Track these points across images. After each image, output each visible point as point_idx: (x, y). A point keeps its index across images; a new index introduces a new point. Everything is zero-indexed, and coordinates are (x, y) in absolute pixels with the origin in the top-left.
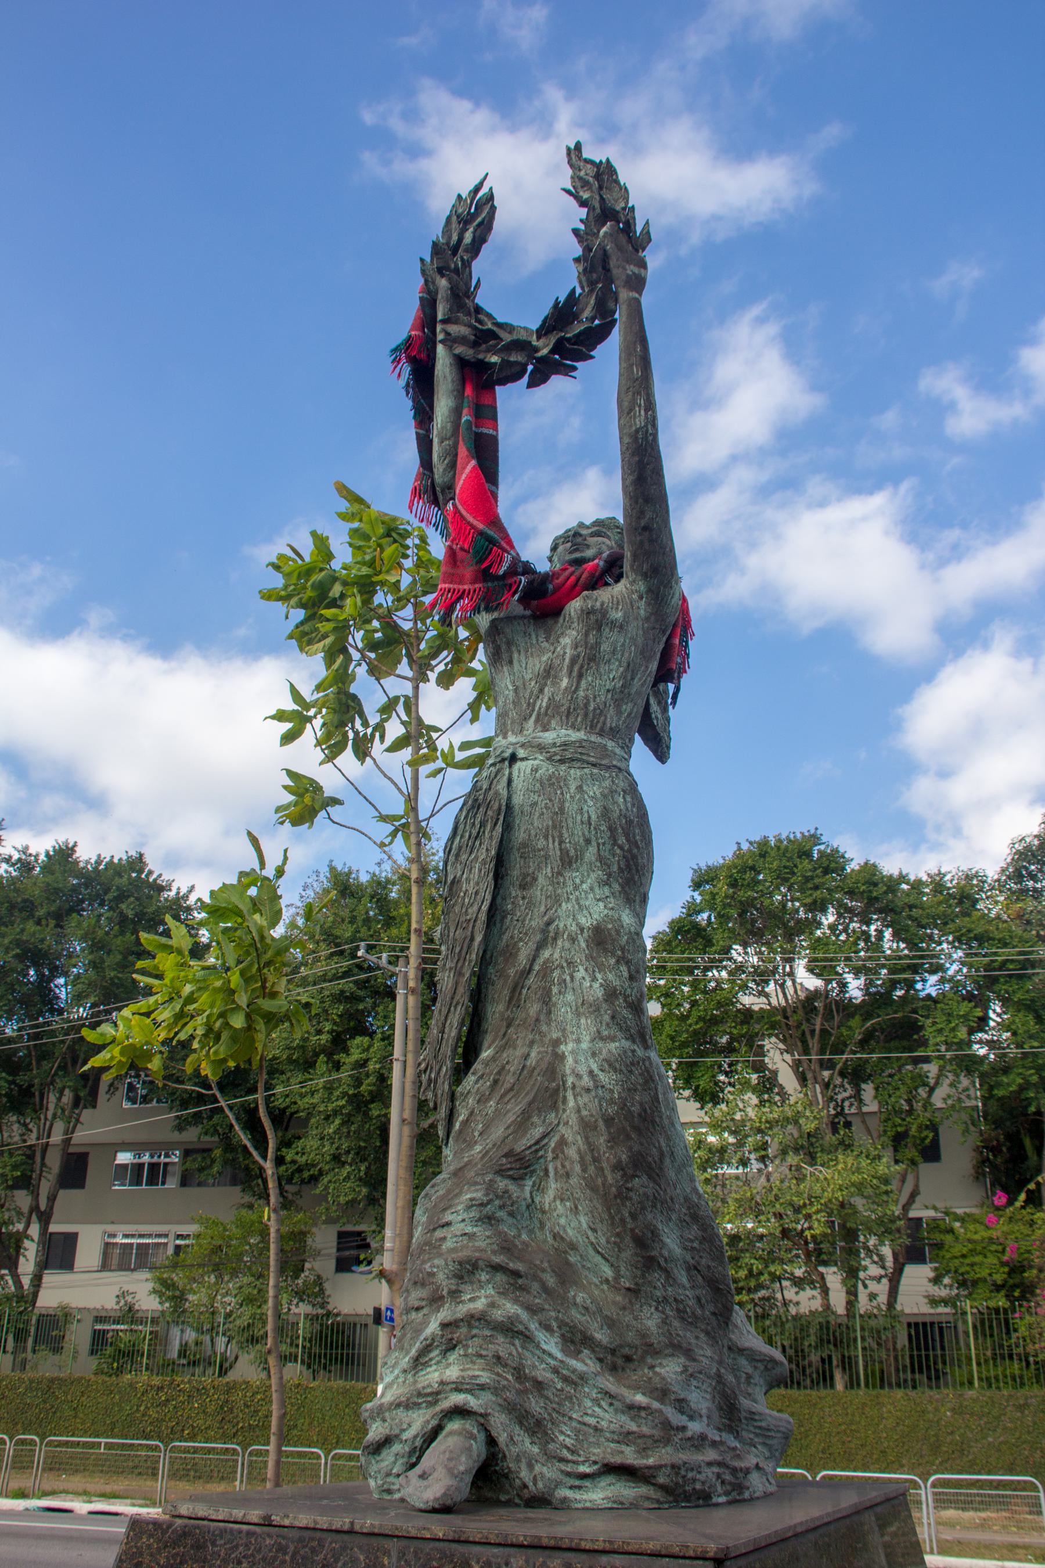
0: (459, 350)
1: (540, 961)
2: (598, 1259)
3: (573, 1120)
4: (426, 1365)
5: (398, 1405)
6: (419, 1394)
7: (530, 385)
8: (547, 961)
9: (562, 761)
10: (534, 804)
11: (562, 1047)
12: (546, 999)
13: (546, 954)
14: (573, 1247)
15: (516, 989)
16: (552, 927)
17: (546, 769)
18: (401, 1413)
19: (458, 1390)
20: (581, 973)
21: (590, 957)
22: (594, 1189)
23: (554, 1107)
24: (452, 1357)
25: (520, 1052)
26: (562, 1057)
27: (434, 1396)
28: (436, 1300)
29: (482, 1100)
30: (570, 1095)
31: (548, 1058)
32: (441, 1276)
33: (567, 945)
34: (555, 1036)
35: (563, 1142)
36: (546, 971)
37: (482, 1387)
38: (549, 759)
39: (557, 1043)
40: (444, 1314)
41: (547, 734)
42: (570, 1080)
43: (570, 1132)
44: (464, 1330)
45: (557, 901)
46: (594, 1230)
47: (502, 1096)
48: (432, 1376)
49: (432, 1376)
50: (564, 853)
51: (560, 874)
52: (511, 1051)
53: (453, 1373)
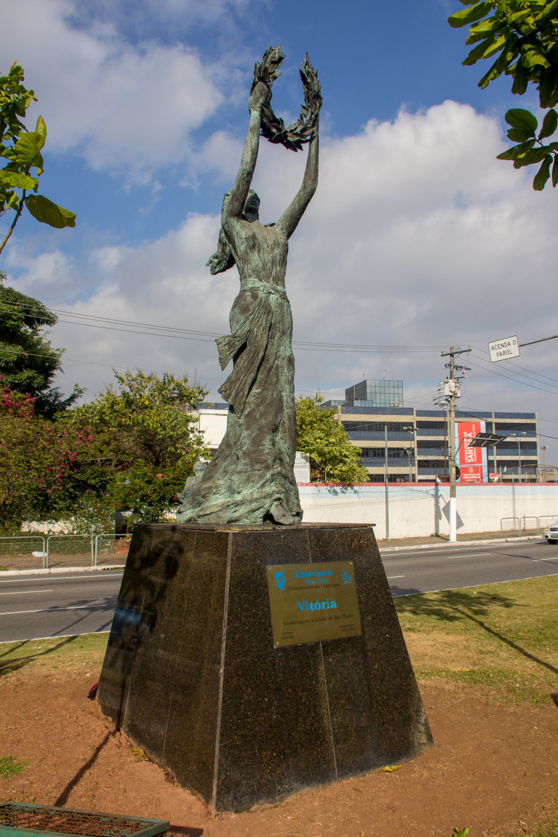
0: (265, 120)
1: (275, 364)
2: (287, 457)
3: (286, 416)
4: (265, 486)
5: (262, 498)
6: (268, 495)
7: (268, 140)
8: (277, 365)
9: (283, 298)
10: (277, 311)
11: (282, 393)
12: (278, 377)
13: (276, 362)
14: (282, 453)
15: (270, 370)
16: (278, 354)
17: (280, 300)
18: (263, 500)
19: (277, 493)
20: (286, 371)
21: (288, 366)
22: (290, 437)
23: (282, 412)
24: (272, 484)
25: (270, 393)
26: (282, 396)
27: (270, 495)
28: (268, 468)
29: (258, 406)
30: (285, 409)
31: (279, 396)
32: (270, 461)
33: (282, 360)
34: (280, 389)
35: (284, 422)
36: (277, 368)
37: (283, 492)
38: (280, 296)
39: (281, 392)
40: (271, 472)
41: (278, 287)
42: (285, 404)
43: (285, 419)
44: (276, 476)
45: (280, 345)
46: (289, 449)
47: (267, 406)
48: (267, 489)
49: (267, 489)
50: (283, 330)
51: (281, 337)
52: (267, 391)
53: (274, 488)
